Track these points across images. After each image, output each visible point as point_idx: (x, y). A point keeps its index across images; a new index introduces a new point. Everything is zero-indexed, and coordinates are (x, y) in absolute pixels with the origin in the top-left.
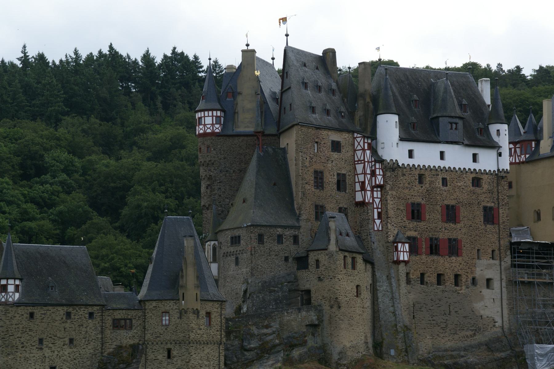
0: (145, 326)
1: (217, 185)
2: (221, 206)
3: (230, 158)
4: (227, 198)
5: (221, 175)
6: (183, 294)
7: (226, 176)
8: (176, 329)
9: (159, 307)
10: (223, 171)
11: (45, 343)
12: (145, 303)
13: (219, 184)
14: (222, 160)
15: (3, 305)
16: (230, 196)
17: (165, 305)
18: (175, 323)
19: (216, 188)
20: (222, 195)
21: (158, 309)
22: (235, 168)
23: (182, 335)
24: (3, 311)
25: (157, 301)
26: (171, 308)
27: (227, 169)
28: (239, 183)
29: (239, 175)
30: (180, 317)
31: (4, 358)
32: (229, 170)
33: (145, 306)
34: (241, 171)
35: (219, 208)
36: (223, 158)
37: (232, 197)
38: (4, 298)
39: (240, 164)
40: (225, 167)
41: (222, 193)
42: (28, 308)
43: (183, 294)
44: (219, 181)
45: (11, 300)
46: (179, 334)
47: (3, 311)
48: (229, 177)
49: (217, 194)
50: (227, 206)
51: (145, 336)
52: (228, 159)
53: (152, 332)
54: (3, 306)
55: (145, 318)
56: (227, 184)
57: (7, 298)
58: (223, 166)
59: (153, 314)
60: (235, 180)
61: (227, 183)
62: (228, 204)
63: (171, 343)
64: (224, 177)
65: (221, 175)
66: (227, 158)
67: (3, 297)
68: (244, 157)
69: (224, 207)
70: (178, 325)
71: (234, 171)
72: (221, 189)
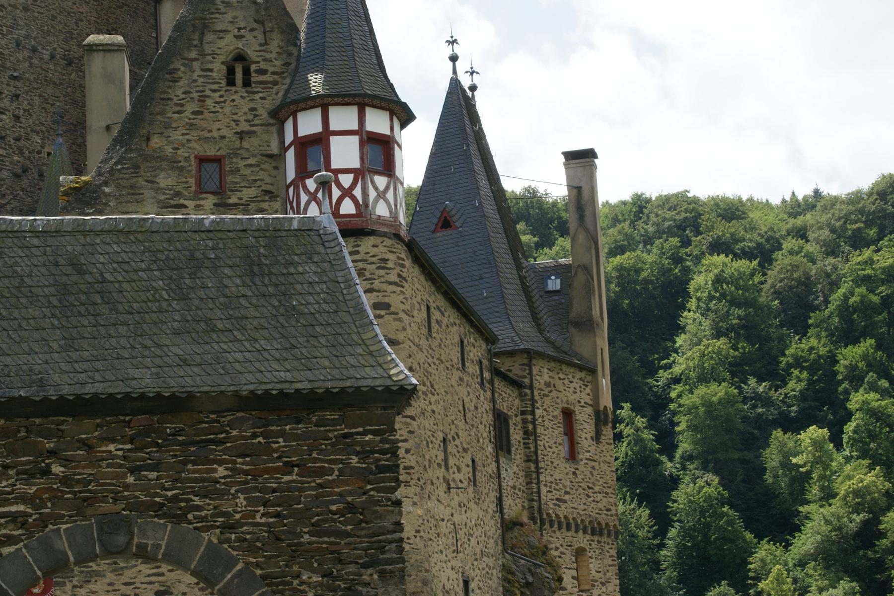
0: (536, 453)
1: (8, 85)
2: (21, 152)
3: (38, 13)
4: (37, 133)
5: (20, 56)
6: (602, 349)
7: (31, 66)
8: (593, 480)
9: (554, 386)
10: (24, 47)
11: (451, 462)
12: (530, 365)
13: (12, 83)
14: (18, 11)
15: (384, 235)
16: (44, 129)
17: (566, 382)
18: (588, 455)
19: (6, 92)
20: (22, 120)
21: (554, 394)
22: (55, 49)
23: (605, 501)
24: (390, 265)
25: (552, 364)
26: (577, 397)
27: (33, 43)
28: (65, 96)
29: (64, 72)
30: (597, 437)
31: (415, 504)
32: (40, 48)
33: (530, 374)
34: (70, 64)
35: (16, 158)
36: (21, 8)
37: (48, 131)
38: (387, 202)
39: (66, 40)
40: (27, 37)
41: (22, 112)
42: (422, 278)
43: (602, 349)
44: (15, 74)
45: (402, 219)
46: (600, 496)
47: (390, 265)
48: (39, 69)
49: (9, 111)
50: (37, 156)
51: (539, 492)
52: (36, 14)
53: (550, 479)
54: (388, 242)
55: (534, 422)
56: (34, 88)
57: (396, 205)
58: (23, 32)
59: (545, 410)
60: (55, 83)
61: (35, 85)
62: (39, 152)
63: (585, 532)
64: (27, 64)
65: (20, 56)
66: (34, 11)
67: (381, 195)
68: (76, 23)
69: (29, 157)
70: (593, 464)
71: (53, 57)
72: (21, 99)
